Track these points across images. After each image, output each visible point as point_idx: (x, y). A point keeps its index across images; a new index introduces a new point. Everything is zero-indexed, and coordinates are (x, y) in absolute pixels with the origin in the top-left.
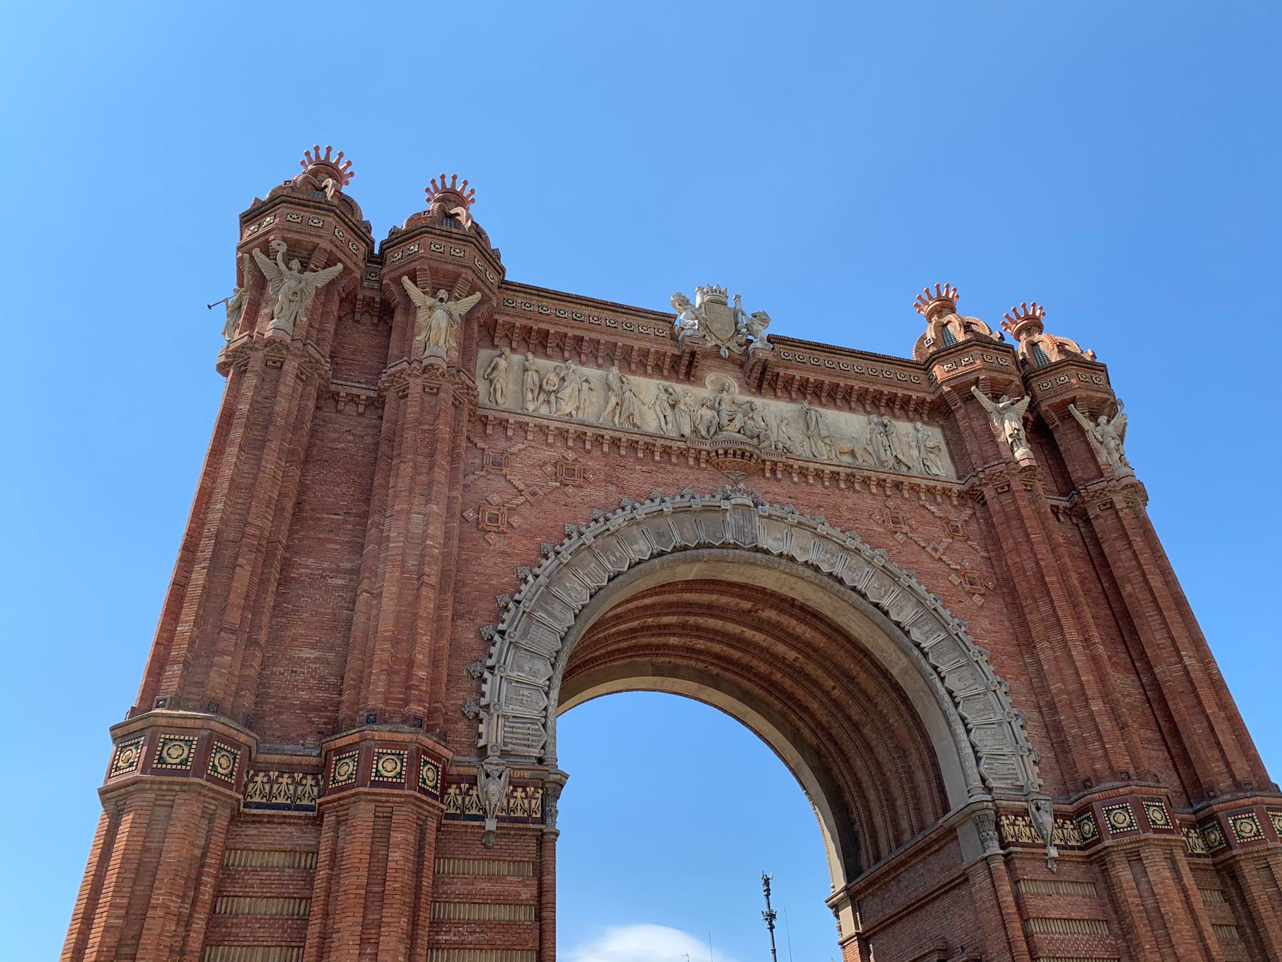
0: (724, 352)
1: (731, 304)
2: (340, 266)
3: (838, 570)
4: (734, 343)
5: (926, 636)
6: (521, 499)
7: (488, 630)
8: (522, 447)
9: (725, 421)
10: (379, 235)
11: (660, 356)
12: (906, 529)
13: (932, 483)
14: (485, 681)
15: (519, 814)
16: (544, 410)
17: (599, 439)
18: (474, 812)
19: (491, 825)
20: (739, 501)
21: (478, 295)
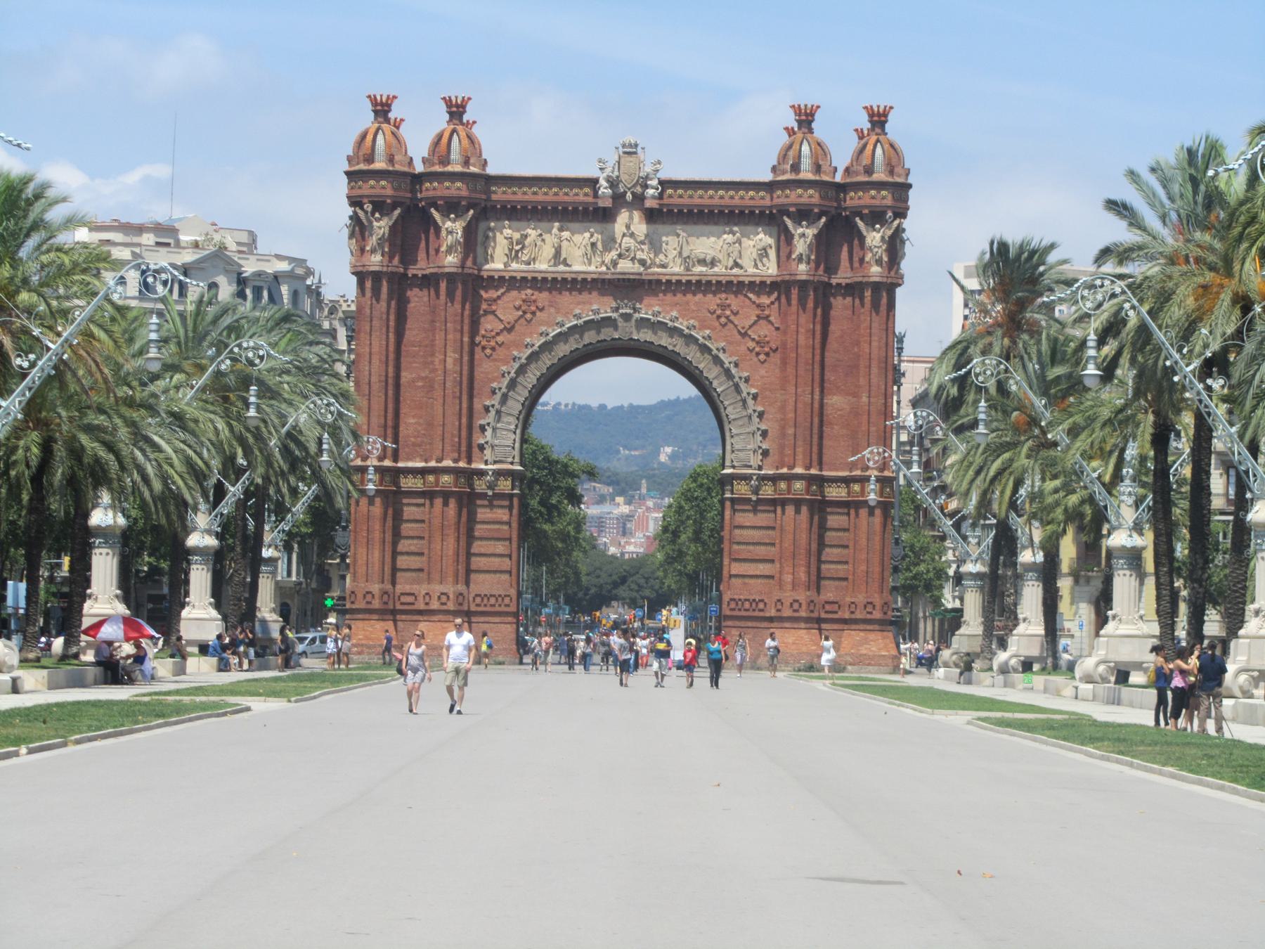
0: (629, 196)
1: (639, 150)
3: (677, 349)
5: (720, 384)
7: (488, 403)
12: (728, 313)
16: (514, 266)
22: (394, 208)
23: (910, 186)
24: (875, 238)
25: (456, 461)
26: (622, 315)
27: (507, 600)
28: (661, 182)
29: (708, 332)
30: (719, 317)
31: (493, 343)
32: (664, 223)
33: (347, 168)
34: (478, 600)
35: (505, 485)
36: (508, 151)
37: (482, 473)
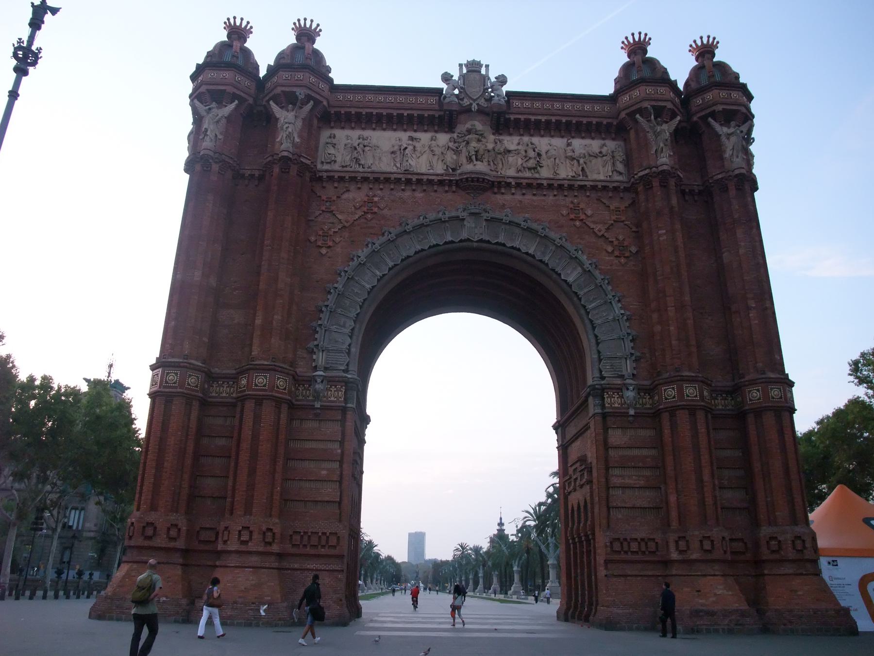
0: (475, 107)
1: (483, 71)
4: (483, 100)
7: (320, 303)
10: (263, 72)
12: (583, 217)
14: (317, 332)
15: (332, 399)
18: (311, 398)
20: (472, 211)
21: (312, 102)
26: (472, 214)
28: (509, 94)
30: (572, 219)
31: (330, 244)
32: (510, 135)
34: (297, 538)
35: (335, 396)
36: (352, 64)
37: (311, 381)
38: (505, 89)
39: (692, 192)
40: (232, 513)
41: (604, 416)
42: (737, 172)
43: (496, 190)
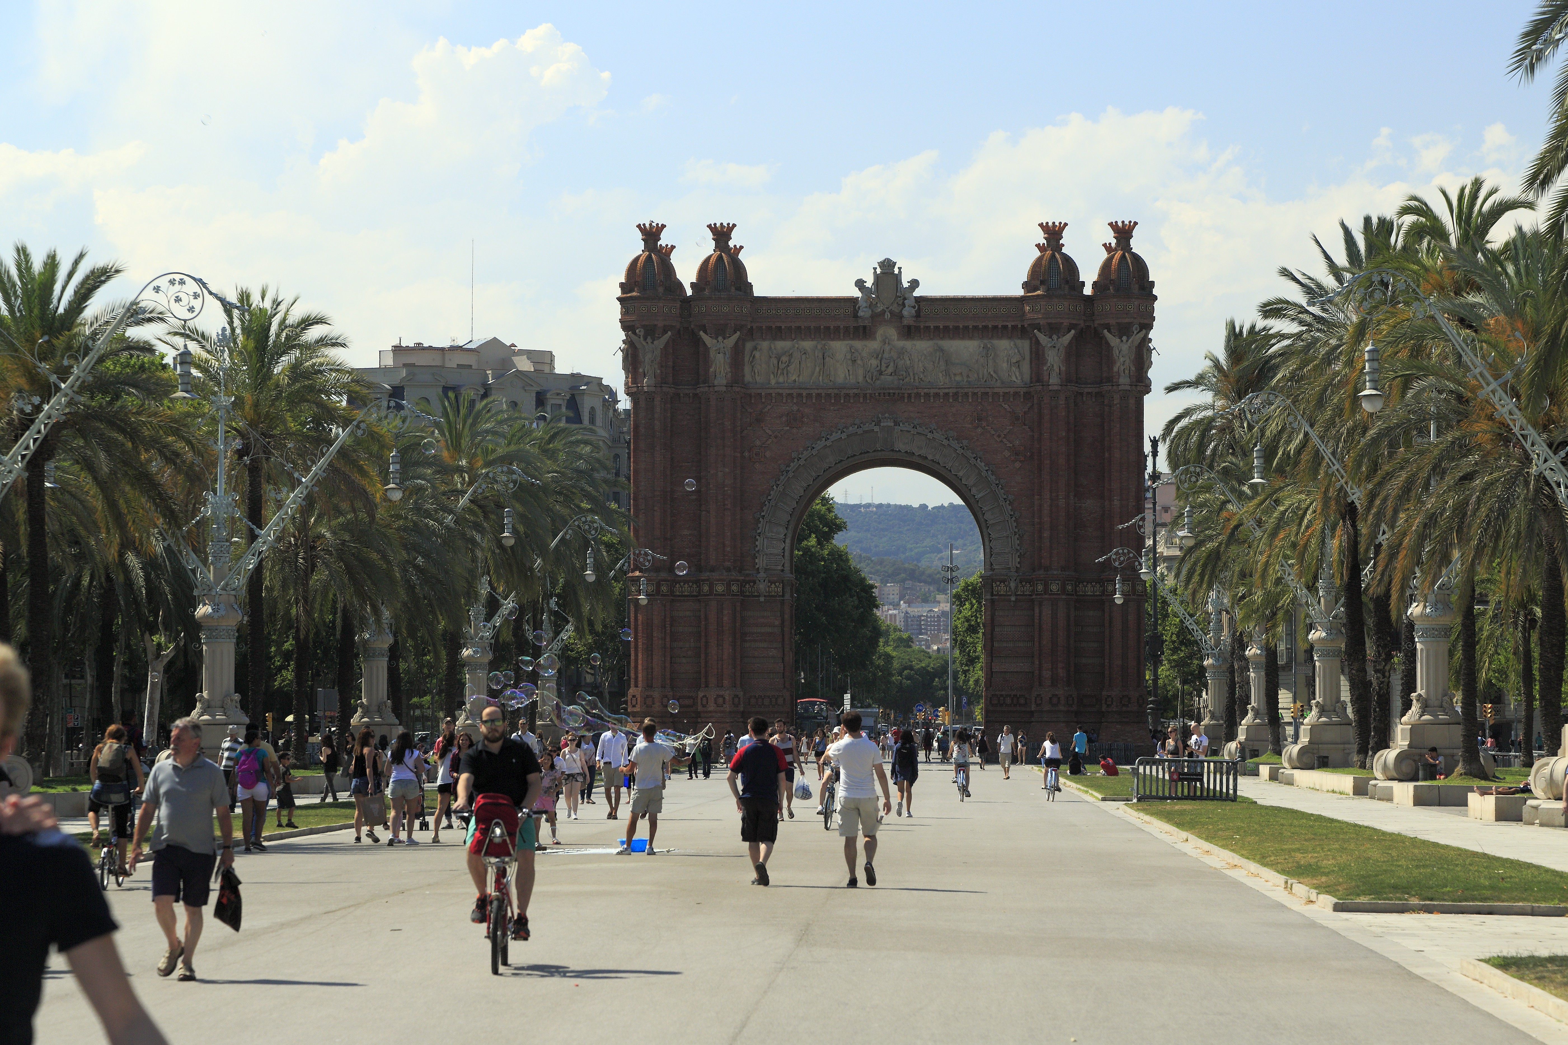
0: (888, 315)
1: (896, 271)
2: (669, 333)
4: (895, 305)
6: (770, 440)
8: (769, 407)
9: (883, 369)
11: (847, 329)
13: (1007, 390)
17: (809, 396)
19: (762, 599)
20: (885, 424)
21: (738, 333)
22: (665, 332)
23: (1155, 298)
24: (1121, 349)
25: (728, 570)
27: (780, 701)
29: (965, 442)
32: (922, 339)
33: (618, 292)
38: (917, 293)
39: (1088, 393)
40: (707, 686)
41: (993, 602)
42: (1121, 388)
43: (906, 401)
